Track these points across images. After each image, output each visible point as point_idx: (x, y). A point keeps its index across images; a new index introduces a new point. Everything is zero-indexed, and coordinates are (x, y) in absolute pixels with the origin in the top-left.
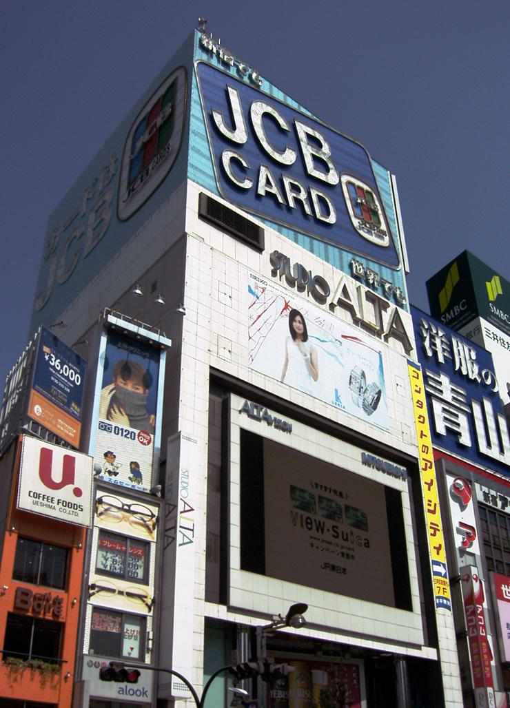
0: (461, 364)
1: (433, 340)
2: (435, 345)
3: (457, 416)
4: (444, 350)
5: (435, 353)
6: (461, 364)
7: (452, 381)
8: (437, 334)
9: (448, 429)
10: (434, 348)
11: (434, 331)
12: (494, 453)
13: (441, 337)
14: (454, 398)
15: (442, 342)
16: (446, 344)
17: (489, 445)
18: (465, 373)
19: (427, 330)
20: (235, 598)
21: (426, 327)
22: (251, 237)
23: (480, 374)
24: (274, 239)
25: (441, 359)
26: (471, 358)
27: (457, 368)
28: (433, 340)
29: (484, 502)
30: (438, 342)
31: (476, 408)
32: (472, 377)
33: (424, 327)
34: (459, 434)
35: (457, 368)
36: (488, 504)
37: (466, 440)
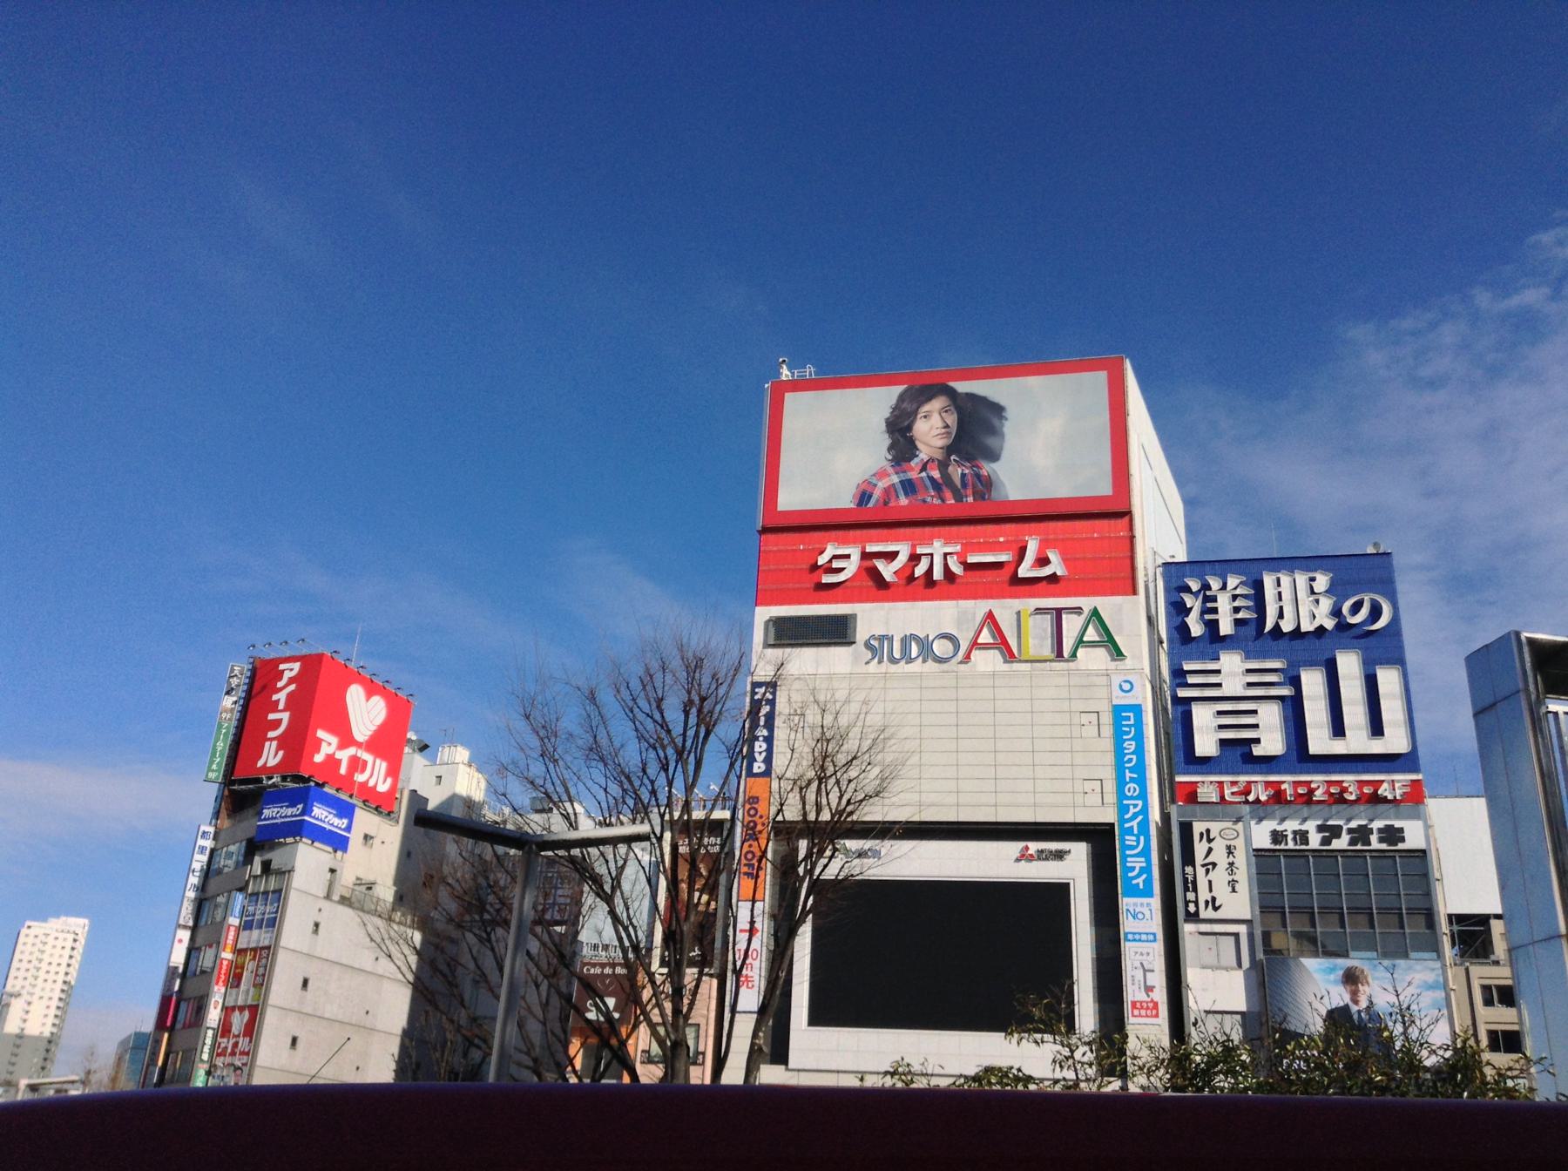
0: (1281, 616)
1: (1209, 605)
2: (1215, 611)
3: (1255, 712)
4: (1237, 610)
5: (1212, 626)
6: (1281, 616)
7: (1248, 656)
8: (1224, 587)
9: (1223, 743)
10: (1207, 617)
11: (1215, 584)
12: (1358, 741)
13: (1235, 588)
14: (1250, 685)
15: (1235, 597)
16: (1245, 596)
17: (1338, 729)
18: (1287, 626)
19: (1196, 594)
20: (794, 1061)
21: (1195, 586)
22: (836, 632)
23: (1336, 612)
24: (871, 618)
25: (1226, 628)
26: (1313, 592)
27: (1269, 625)
28: (1209, 605)
29: (1272, 847)
30: (1224, 604)
31: (1313, 682)
32: (1306, 626)
33: (1188, 589)
34: (1257, 741)
35: (1269, 625)
36: (1282, 847)
37: (1272, 742)
